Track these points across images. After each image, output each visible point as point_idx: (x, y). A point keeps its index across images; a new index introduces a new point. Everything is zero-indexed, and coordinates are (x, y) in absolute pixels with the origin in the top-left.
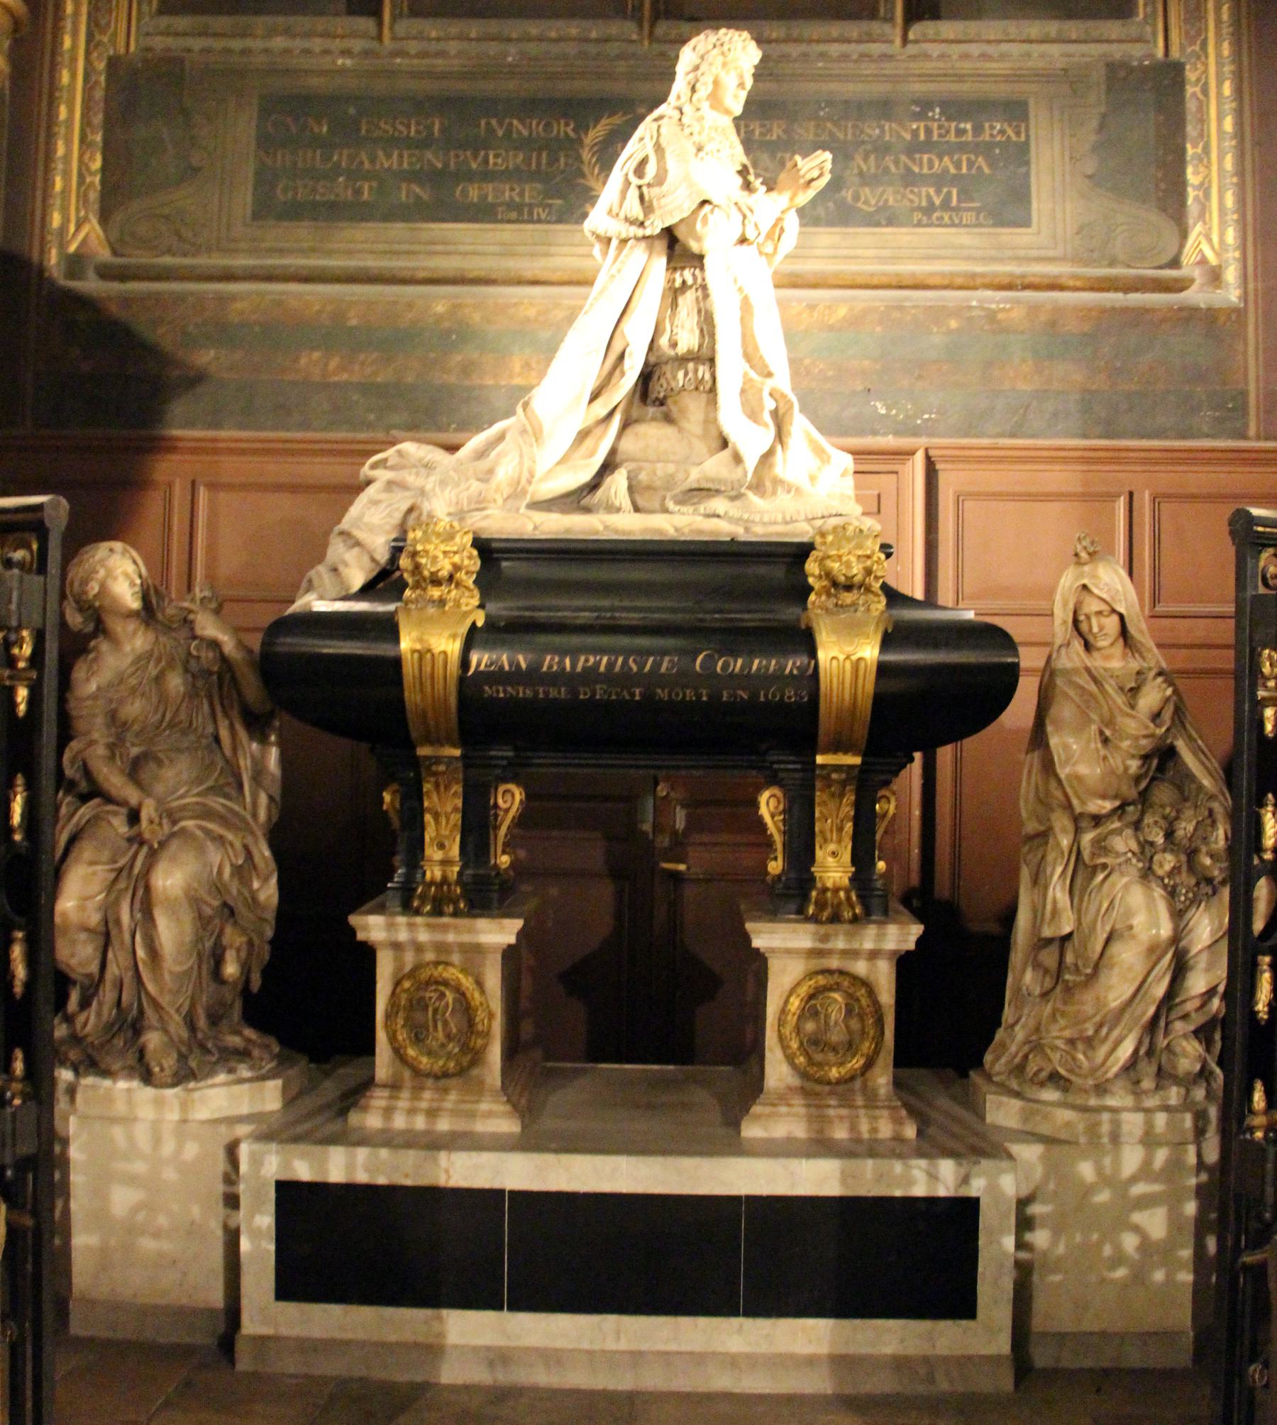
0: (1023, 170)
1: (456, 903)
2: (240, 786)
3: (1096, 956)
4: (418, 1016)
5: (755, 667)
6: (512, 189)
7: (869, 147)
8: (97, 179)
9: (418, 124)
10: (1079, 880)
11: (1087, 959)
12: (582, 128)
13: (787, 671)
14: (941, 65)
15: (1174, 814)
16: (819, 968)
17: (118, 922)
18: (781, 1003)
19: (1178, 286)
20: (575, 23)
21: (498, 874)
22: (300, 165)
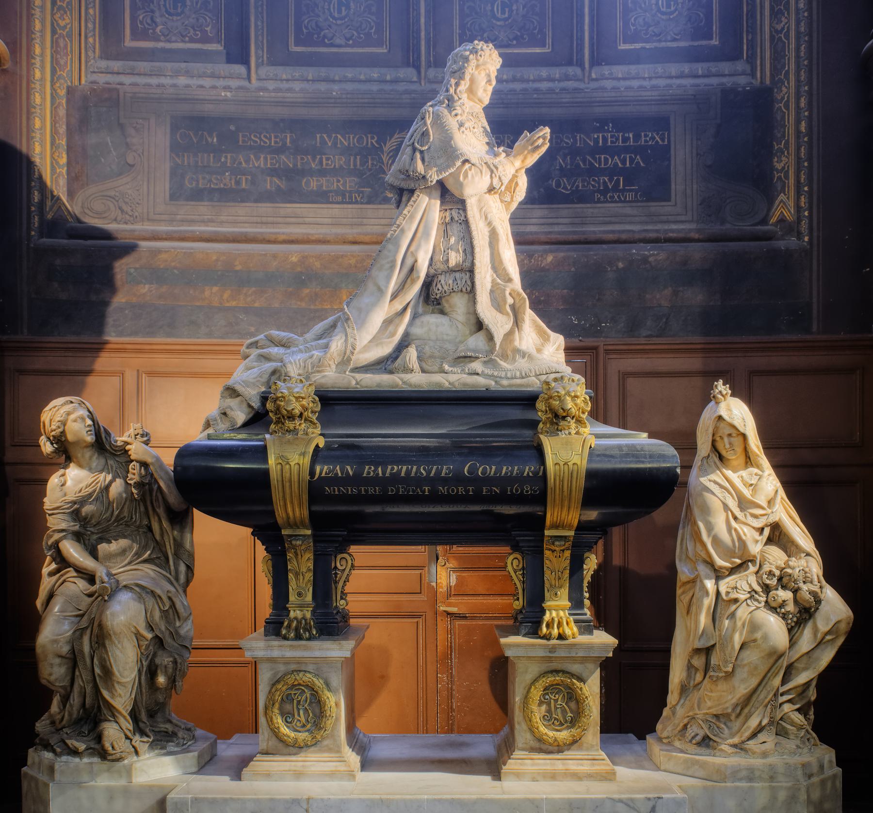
0: (666, 163)
1: (310, 631)
2: (167, 559)
4: (288, 707)
5: (504, 472)
6: (338, 181)
7: (566, 151)
8: (64, 171)
9: (276, 137)
12: (382, 140)
13: (525, 474)
14: (613, 94)
16: (546, 670)
17: (82, 652)
18: (525, 692)
19: (768, 237)
20: (376, 70)
21: (338, 612)
22: (200, 164)
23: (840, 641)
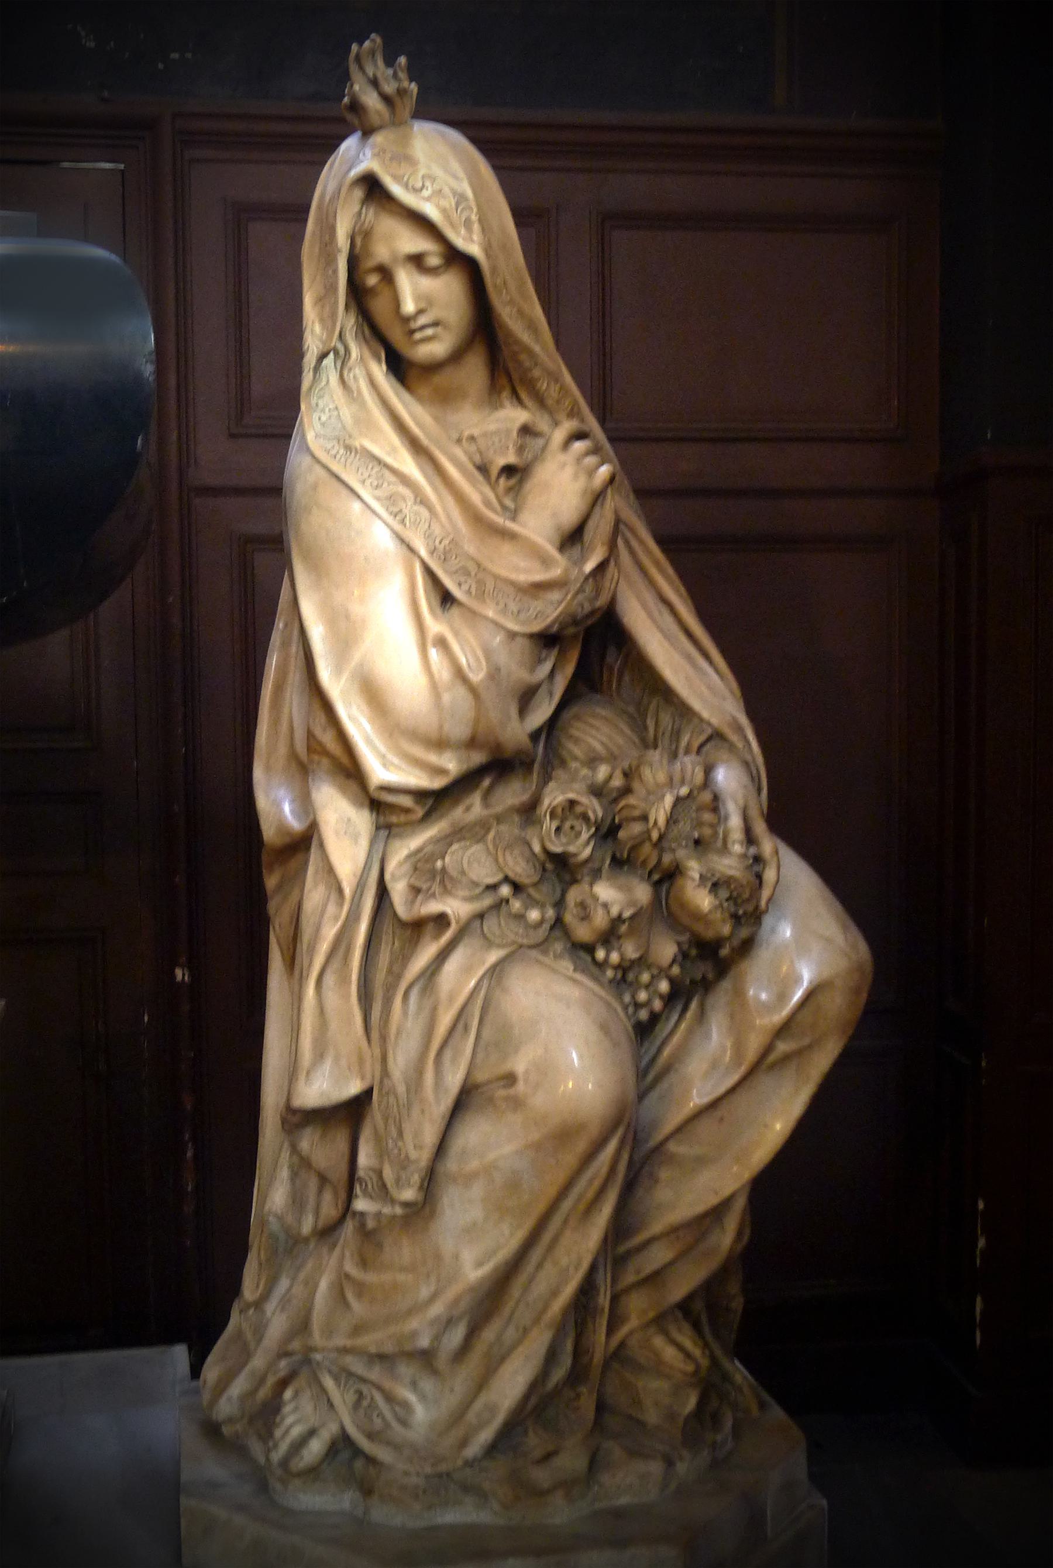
3: (423, 1157)
10: (384, 958)
11: (404, 1164)
15: (617, 782)
23: (823, 1060)
